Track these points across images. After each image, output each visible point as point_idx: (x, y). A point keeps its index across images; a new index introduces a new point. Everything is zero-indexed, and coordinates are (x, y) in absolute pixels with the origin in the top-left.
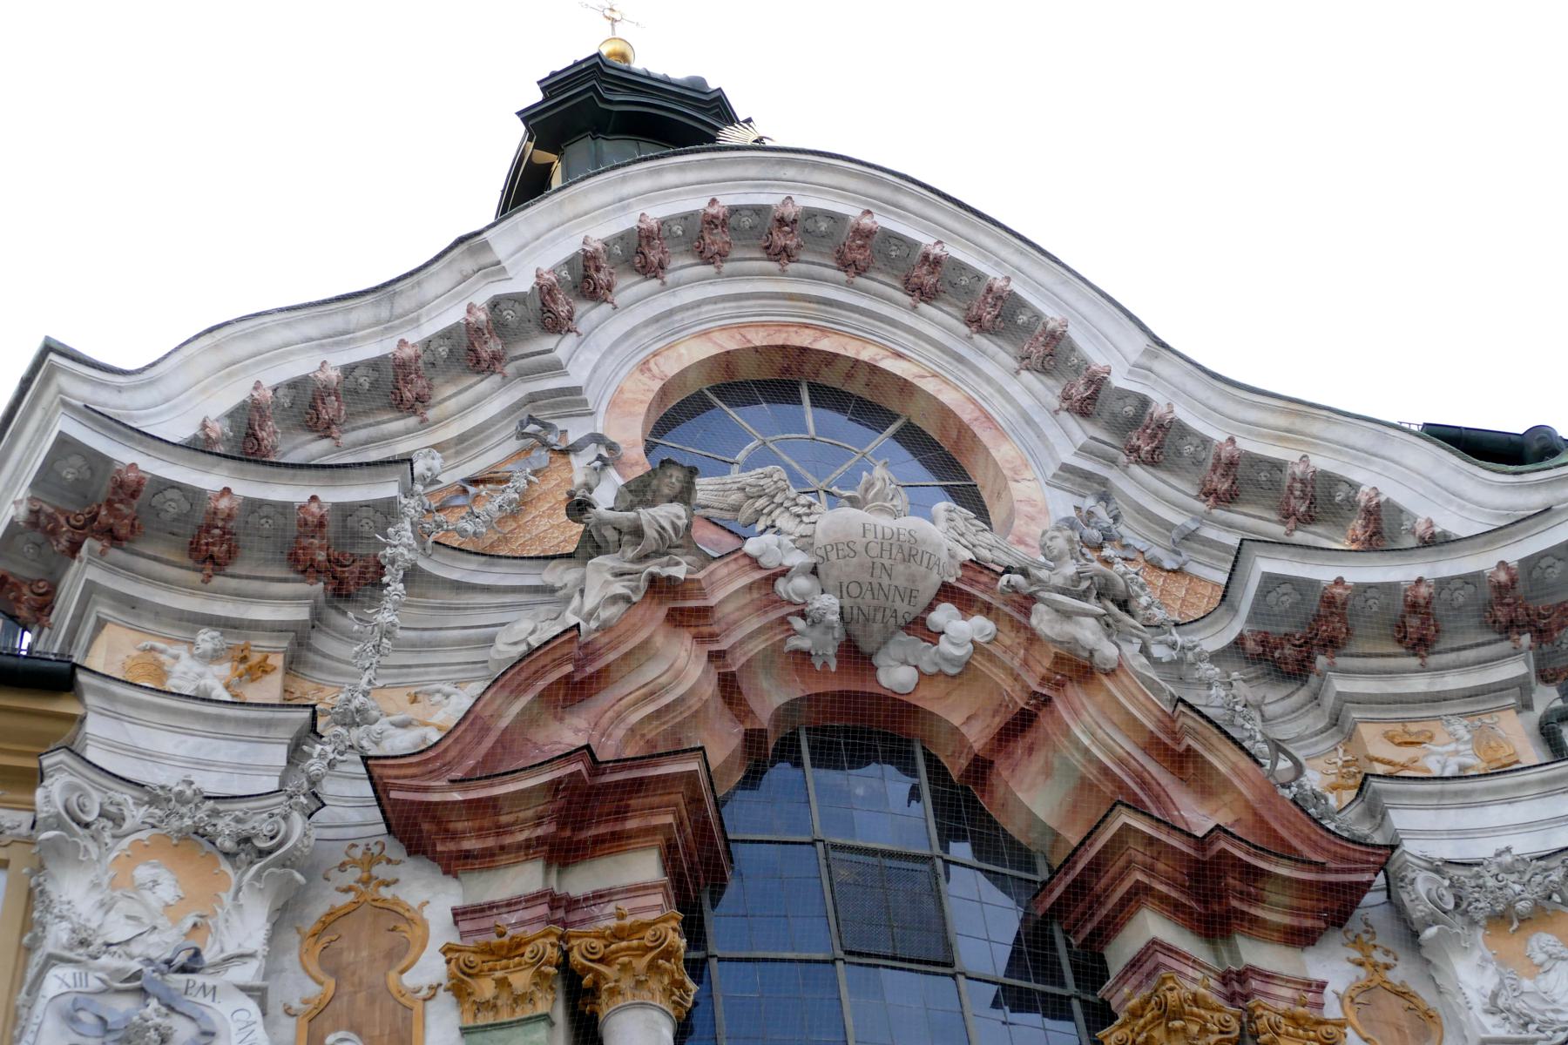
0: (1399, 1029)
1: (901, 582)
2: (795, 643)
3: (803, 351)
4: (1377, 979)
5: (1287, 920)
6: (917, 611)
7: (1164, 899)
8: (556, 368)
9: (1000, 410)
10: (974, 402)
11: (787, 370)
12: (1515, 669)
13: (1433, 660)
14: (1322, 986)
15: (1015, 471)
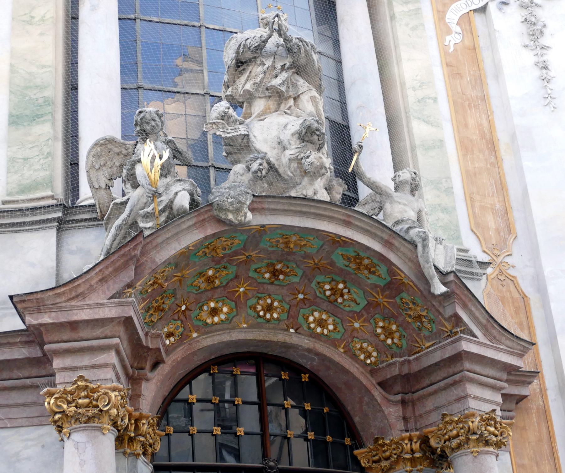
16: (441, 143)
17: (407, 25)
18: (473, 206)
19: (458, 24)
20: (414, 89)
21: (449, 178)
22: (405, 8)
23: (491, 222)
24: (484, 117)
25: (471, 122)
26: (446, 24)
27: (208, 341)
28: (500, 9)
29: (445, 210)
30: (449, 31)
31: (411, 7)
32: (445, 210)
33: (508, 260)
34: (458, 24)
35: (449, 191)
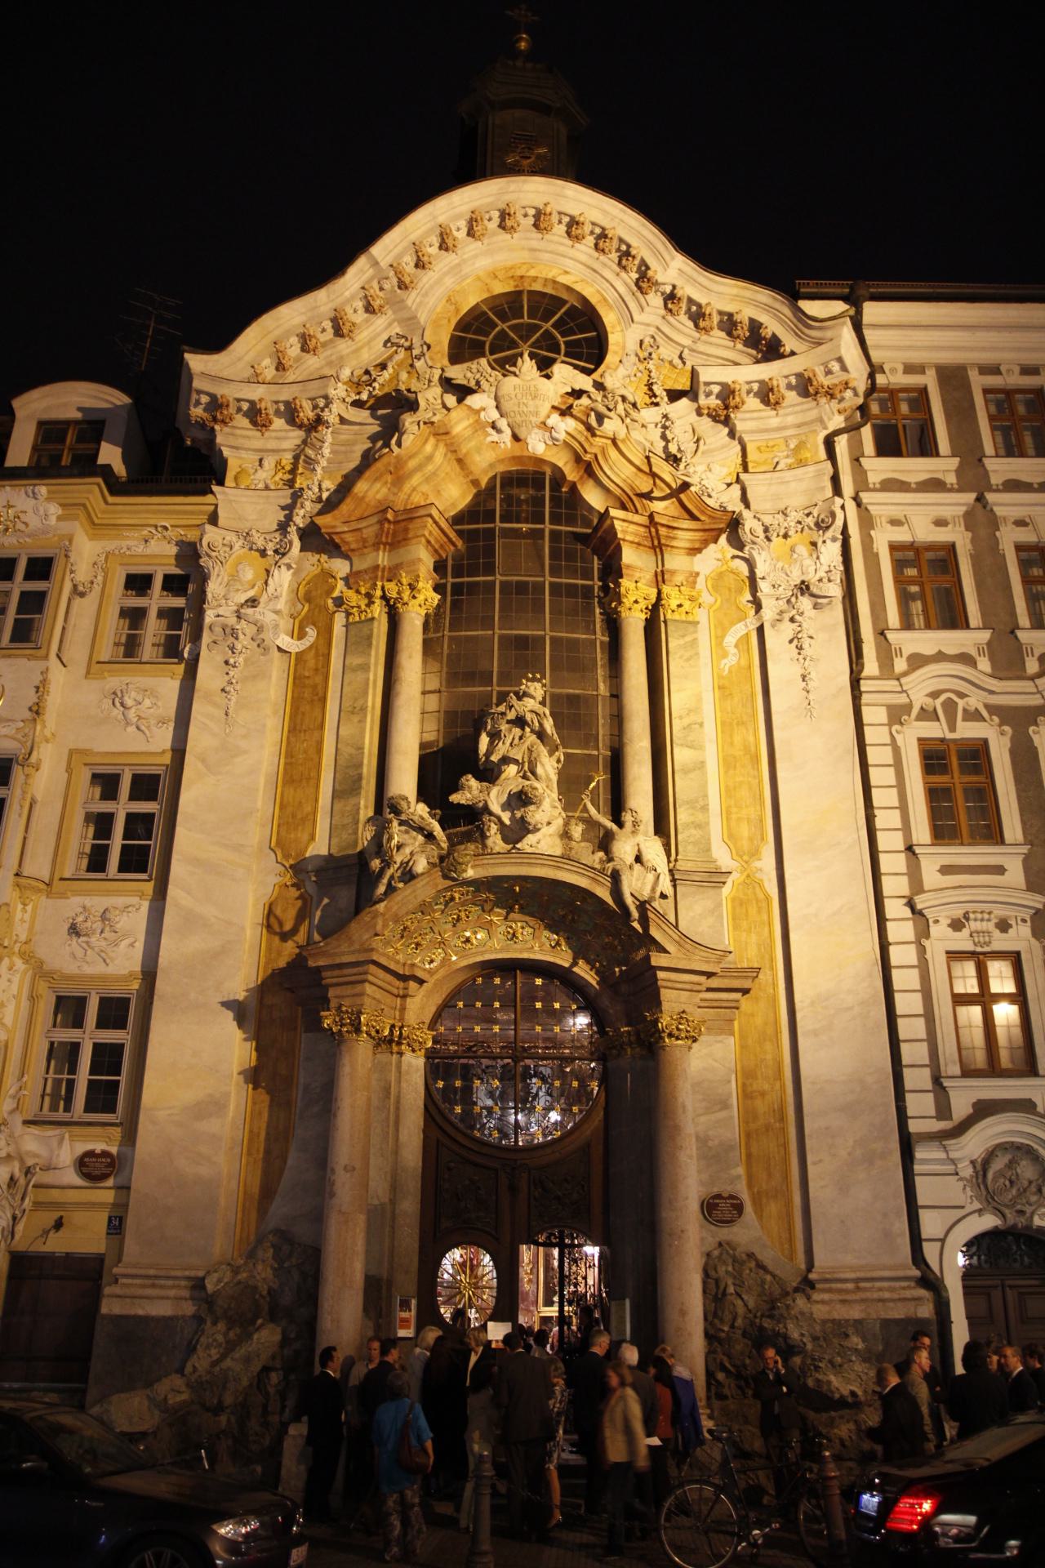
0: (730, 590)
1: (531, 409)
2: (489, 439)
3: (522, 277)
4: (725, 567)
5: (688, 545)
6: (542, 419)
7: (632, 542)
8: (406, 308)
9: (611, 296)
10: (598, 291)
11: (517, 286)
12: (813, 414)
13: (781, 412)
14: (698, 574)
15: (613, 327)
16: (701, 765)
17: (681, 657)
18: (728, 819)
19: (736, 646)
20: (681, 718)
21: (706, 796)
22: (682, 642)
23: (744, 831)
24: (751, 732)
25: (737, 739)
26: (723, 648)
27: (465, 963)
28: (773, 626)
29: (698, 826)
30: (725, 655)
31: (688, 638)
32: (698, 826)
33: (758, 864)
34: (736, 646)
35: (705, 808)
